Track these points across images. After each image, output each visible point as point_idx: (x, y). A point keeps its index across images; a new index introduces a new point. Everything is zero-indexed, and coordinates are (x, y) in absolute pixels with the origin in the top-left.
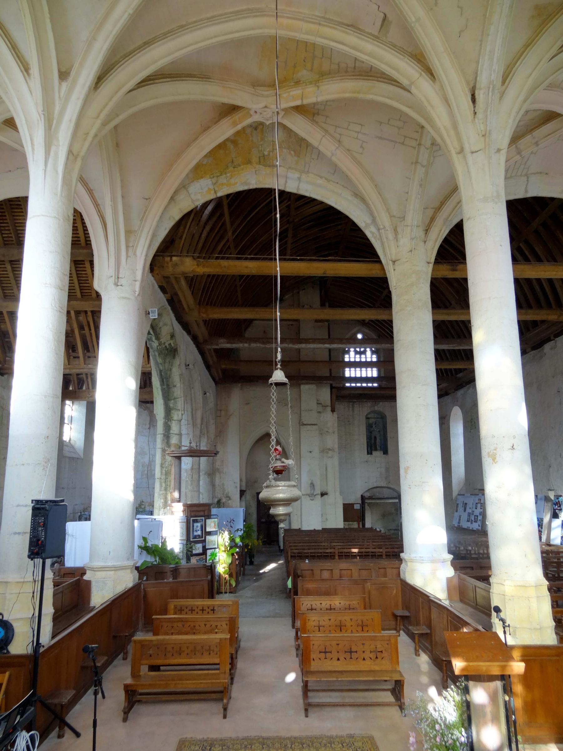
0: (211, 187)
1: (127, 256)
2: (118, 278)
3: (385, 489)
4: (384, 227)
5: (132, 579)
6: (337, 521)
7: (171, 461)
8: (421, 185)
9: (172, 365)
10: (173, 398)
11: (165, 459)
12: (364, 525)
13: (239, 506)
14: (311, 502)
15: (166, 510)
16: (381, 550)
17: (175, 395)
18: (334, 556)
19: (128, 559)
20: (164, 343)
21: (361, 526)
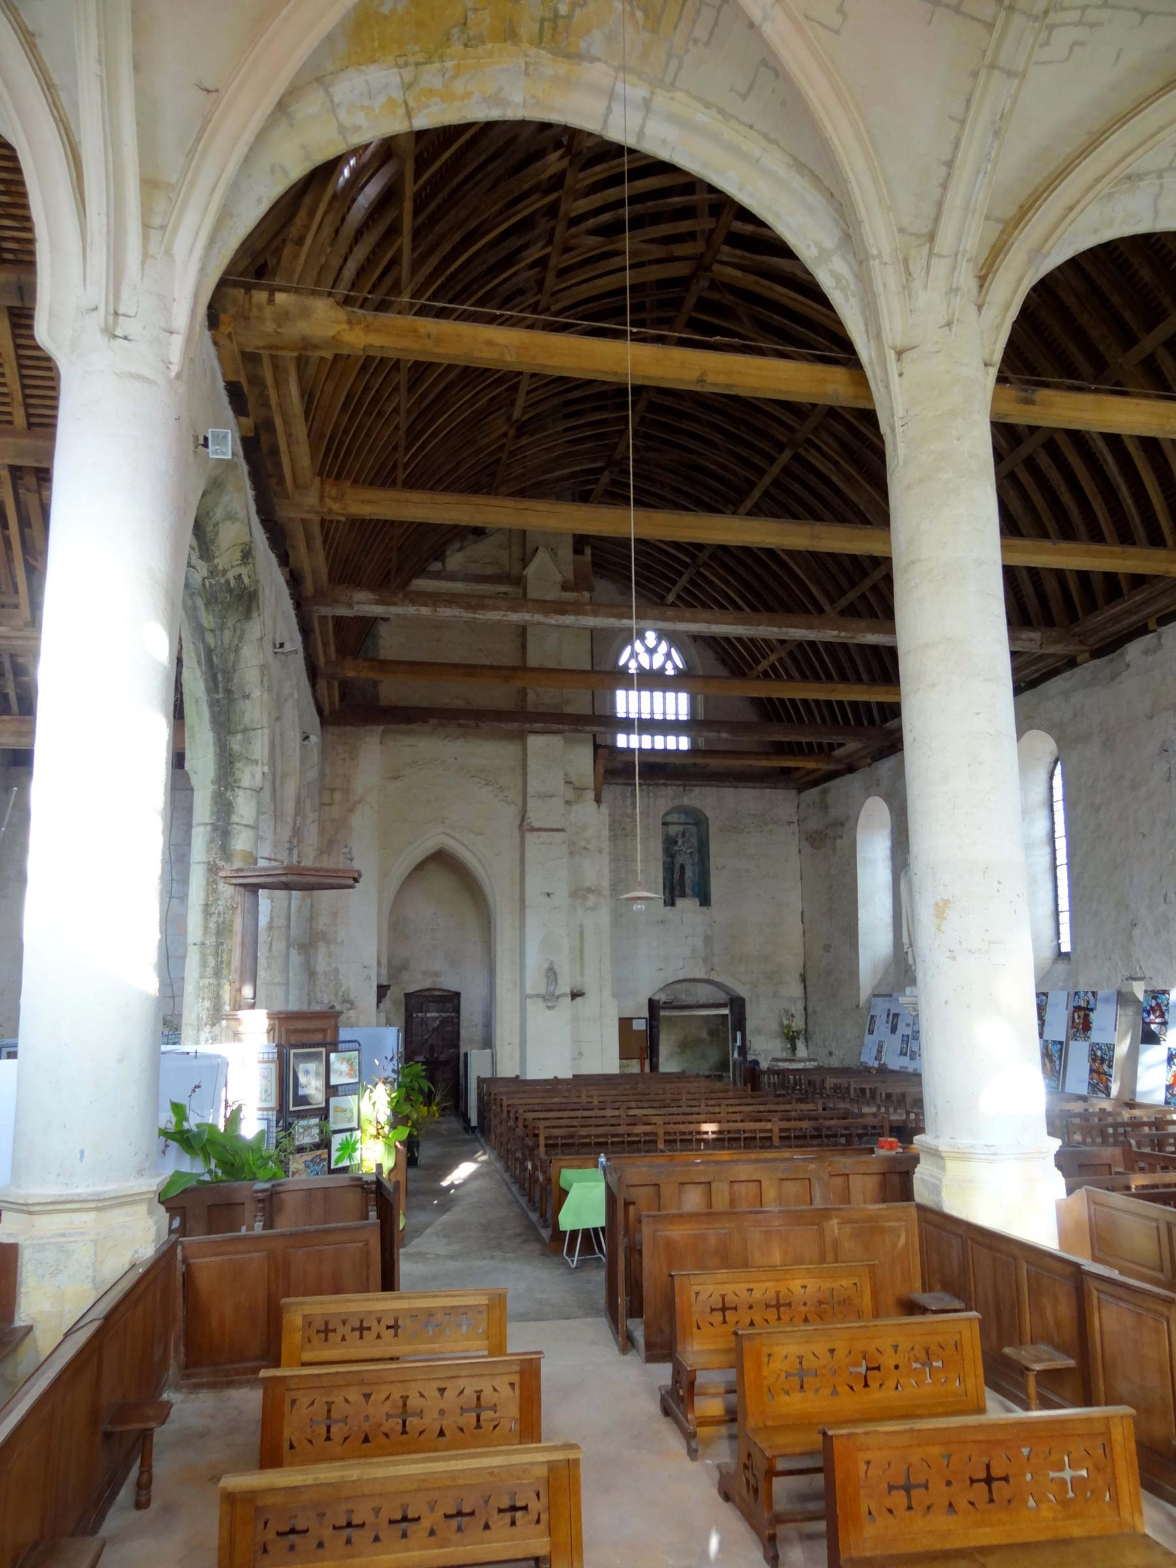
0: (397, 95)
1: (146, 255)
2: (116, 314)
3: (700, 986)
4: (880, 255)
5: (152, 1235)
6: (605, 1059)
7: (232, 897)
8: (997, 133)
9: (241, 638)
10: (241, 727)
11: (215, 891)
12: (654, 1067)
13: (374, 1020)
14: (549, 1013)
15: (217, 1028)
16: (769, 1126)
17: (247, 720)
18: (655, 1142)
19: (140, 1172)
20: (225, 571)
21: (647, 1069)
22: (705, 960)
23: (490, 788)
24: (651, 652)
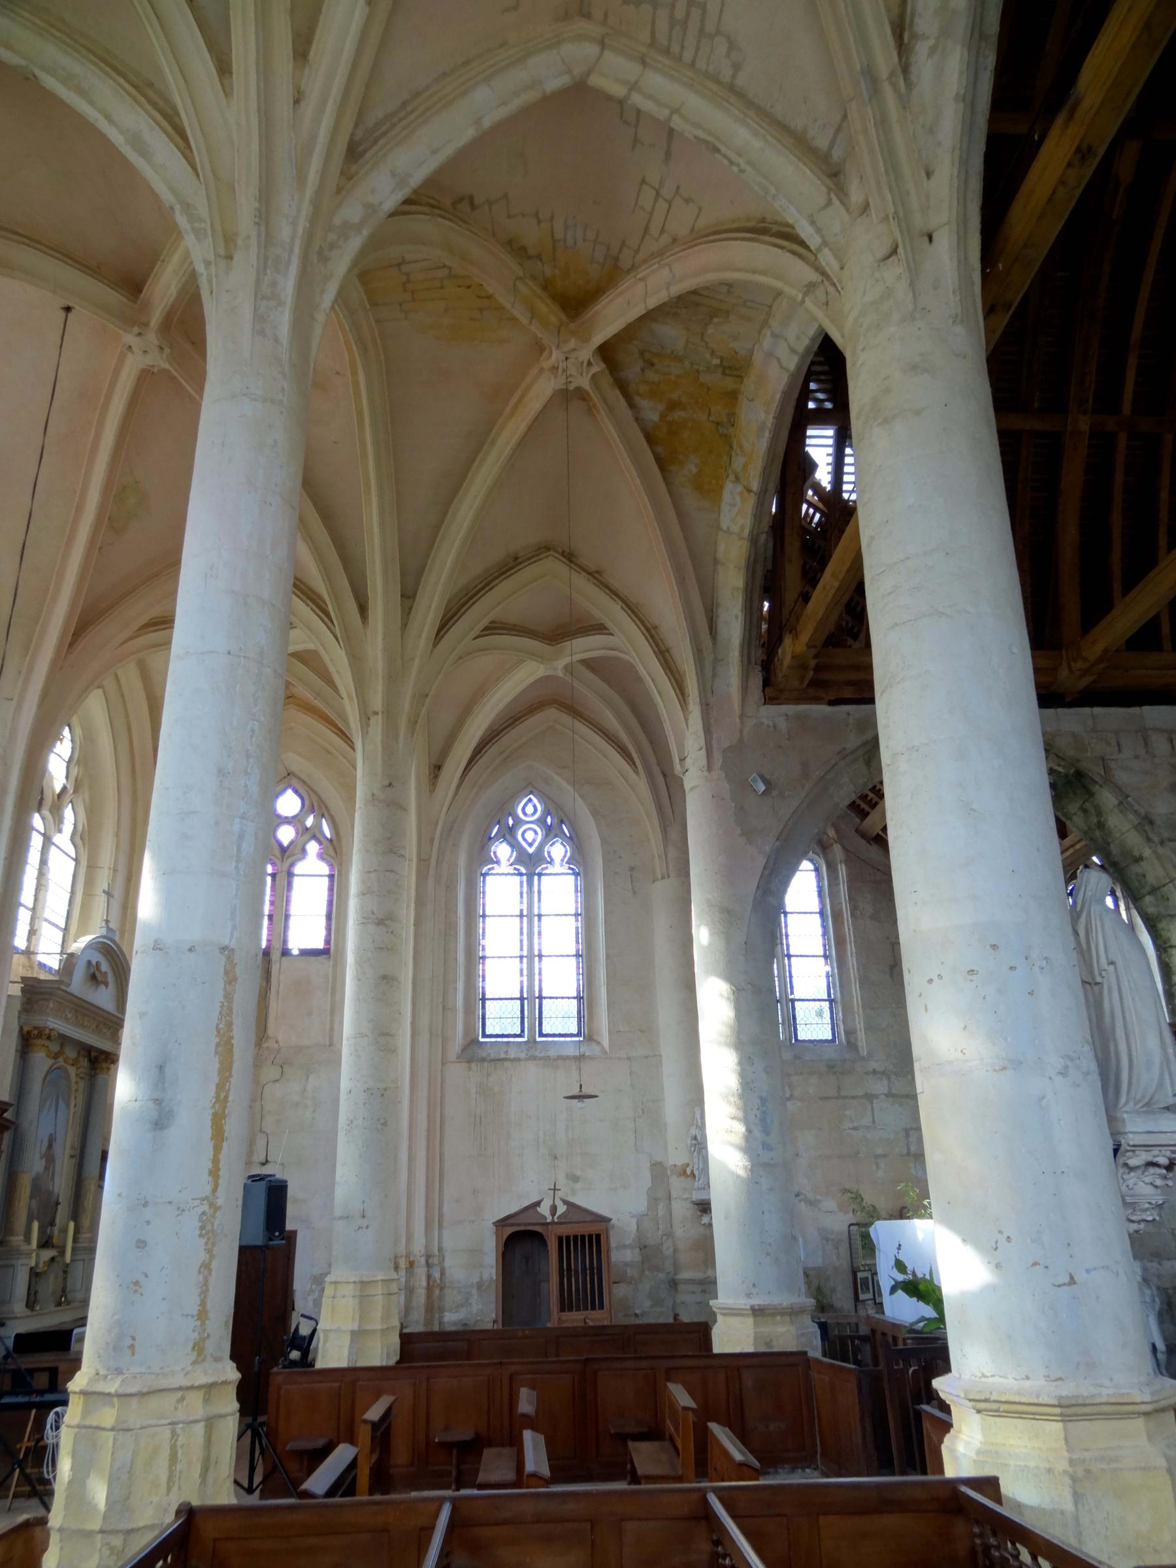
9: (1099, 813)
10: (1148, 888)
17: (1151, 879)
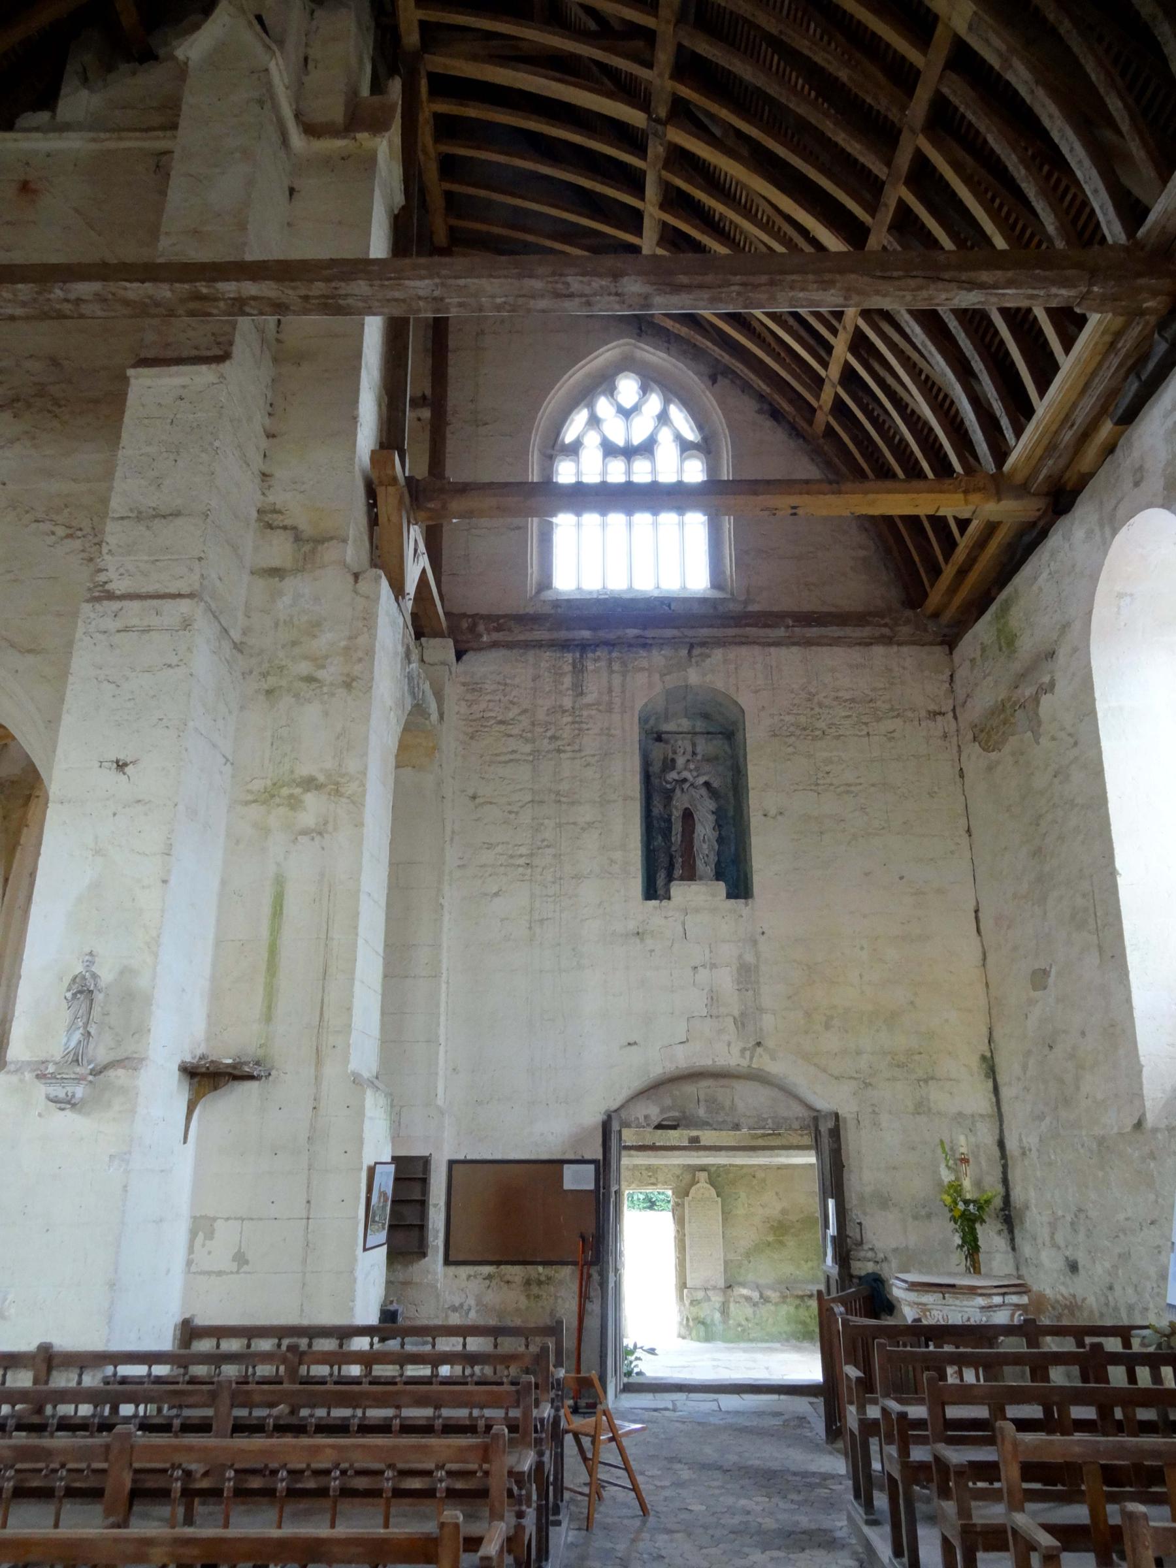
3: (740, 1087)
22: (741, 1022)
23: (77, 544)
24: (626, 414)
